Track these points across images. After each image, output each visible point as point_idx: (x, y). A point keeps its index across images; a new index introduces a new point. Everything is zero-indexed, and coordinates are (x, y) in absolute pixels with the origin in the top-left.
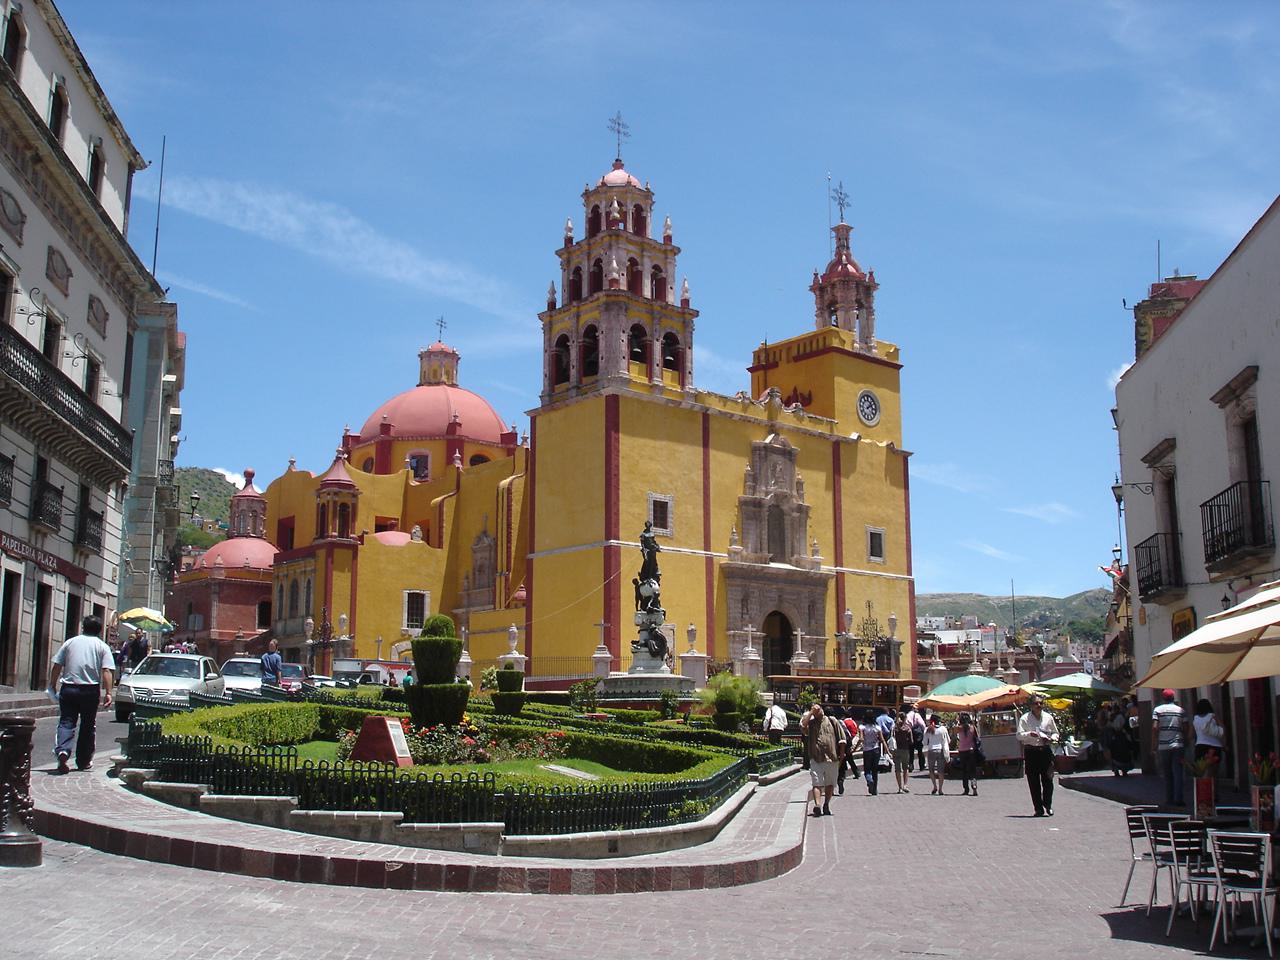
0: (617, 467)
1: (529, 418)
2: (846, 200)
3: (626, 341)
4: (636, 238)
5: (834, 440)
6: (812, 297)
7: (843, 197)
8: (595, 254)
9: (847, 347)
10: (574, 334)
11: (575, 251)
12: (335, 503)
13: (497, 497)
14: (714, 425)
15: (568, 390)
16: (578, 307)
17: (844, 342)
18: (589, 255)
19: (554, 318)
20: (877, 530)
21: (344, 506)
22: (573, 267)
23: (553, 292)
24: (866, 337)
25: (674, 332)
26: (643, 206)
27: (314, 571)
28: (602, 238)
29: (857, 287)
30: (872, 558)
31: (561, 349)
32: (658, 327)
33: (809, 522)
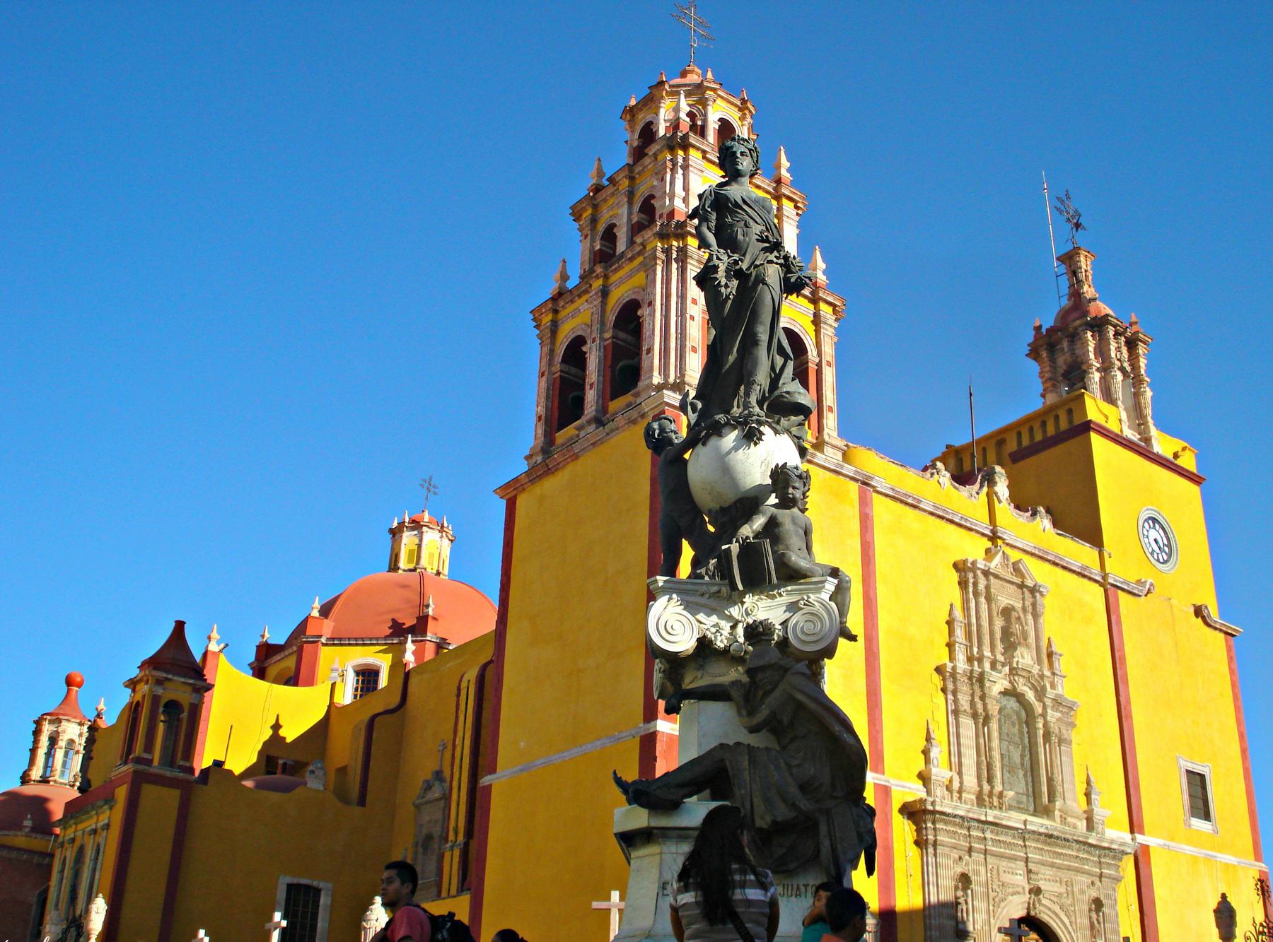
1: (502, 504)
6: (1034, 367)
8: (642, 192)
10: (596, 327)
11: (605, 200)
13: (458, 695)
14: (881, 507)
15: (580, 428)
16: (606, 277)
17: (1107, 417)
18: (631, 195)
19: (562, 314)
21: (173, 707)
22: (601, 228)
23: (564, 277)
25: (796, 330)
27: (107, 826)
28: (655, 156)
29: (1117, 334)
30: (1198, 823)
31: (573, 370)
33: (1075, 736)
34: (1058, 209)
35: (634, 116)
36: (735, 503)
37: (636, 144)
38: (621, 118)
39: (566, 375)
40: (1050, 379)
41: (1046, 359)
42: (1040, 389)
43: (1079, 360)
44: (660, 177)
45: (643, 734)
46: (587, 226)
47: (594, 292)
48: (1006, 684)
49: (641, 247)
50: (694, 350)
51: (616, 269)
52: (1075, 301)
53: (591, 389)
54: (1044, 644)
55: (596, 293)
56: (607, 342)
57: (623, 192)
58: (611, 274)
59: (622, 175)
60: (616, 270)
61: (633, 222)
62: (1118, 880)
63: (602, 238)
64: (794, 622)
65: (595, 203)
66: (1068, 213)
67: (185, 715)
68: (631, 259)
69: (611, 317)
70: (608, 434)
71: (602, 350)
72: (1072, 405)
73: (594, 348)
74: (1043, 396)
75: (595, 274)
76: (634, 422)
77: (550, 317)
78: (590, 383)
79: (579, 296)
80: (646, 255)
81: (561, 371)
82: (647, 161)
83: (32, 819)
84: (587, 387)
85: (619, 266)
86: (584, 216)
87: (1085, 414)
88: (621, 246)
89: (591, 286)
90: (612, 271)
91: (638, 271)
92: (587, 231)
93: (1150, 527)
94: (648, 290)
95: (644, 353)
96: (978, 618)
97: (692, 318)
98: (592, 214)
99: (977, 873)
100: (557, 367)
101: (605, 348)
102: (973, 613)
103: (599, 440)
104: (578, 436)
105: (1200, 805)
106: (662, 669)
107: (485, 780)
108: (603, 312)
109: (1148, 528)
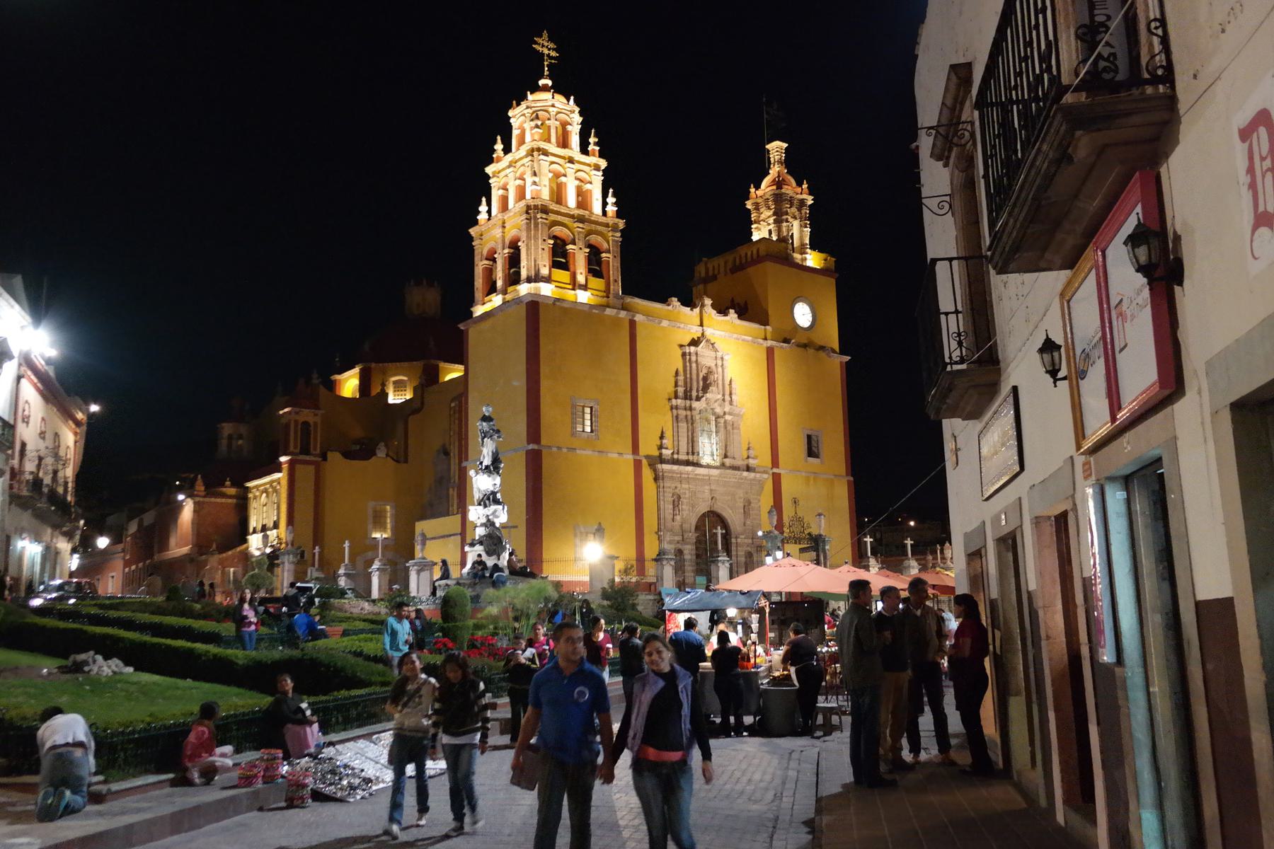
3: (547, 249)
12: (296, 422)
21: (306, 424)
30: (811, 460)
48: (704, 405)
50: (545, 266)
54: (727, 382)
62: (760, 493)
67: (312, 428)
83: (230, 480)
96: (691, 373)
99: (685, 494)
102: (688, 372)
105: (812, 450)
107: (464, 464)
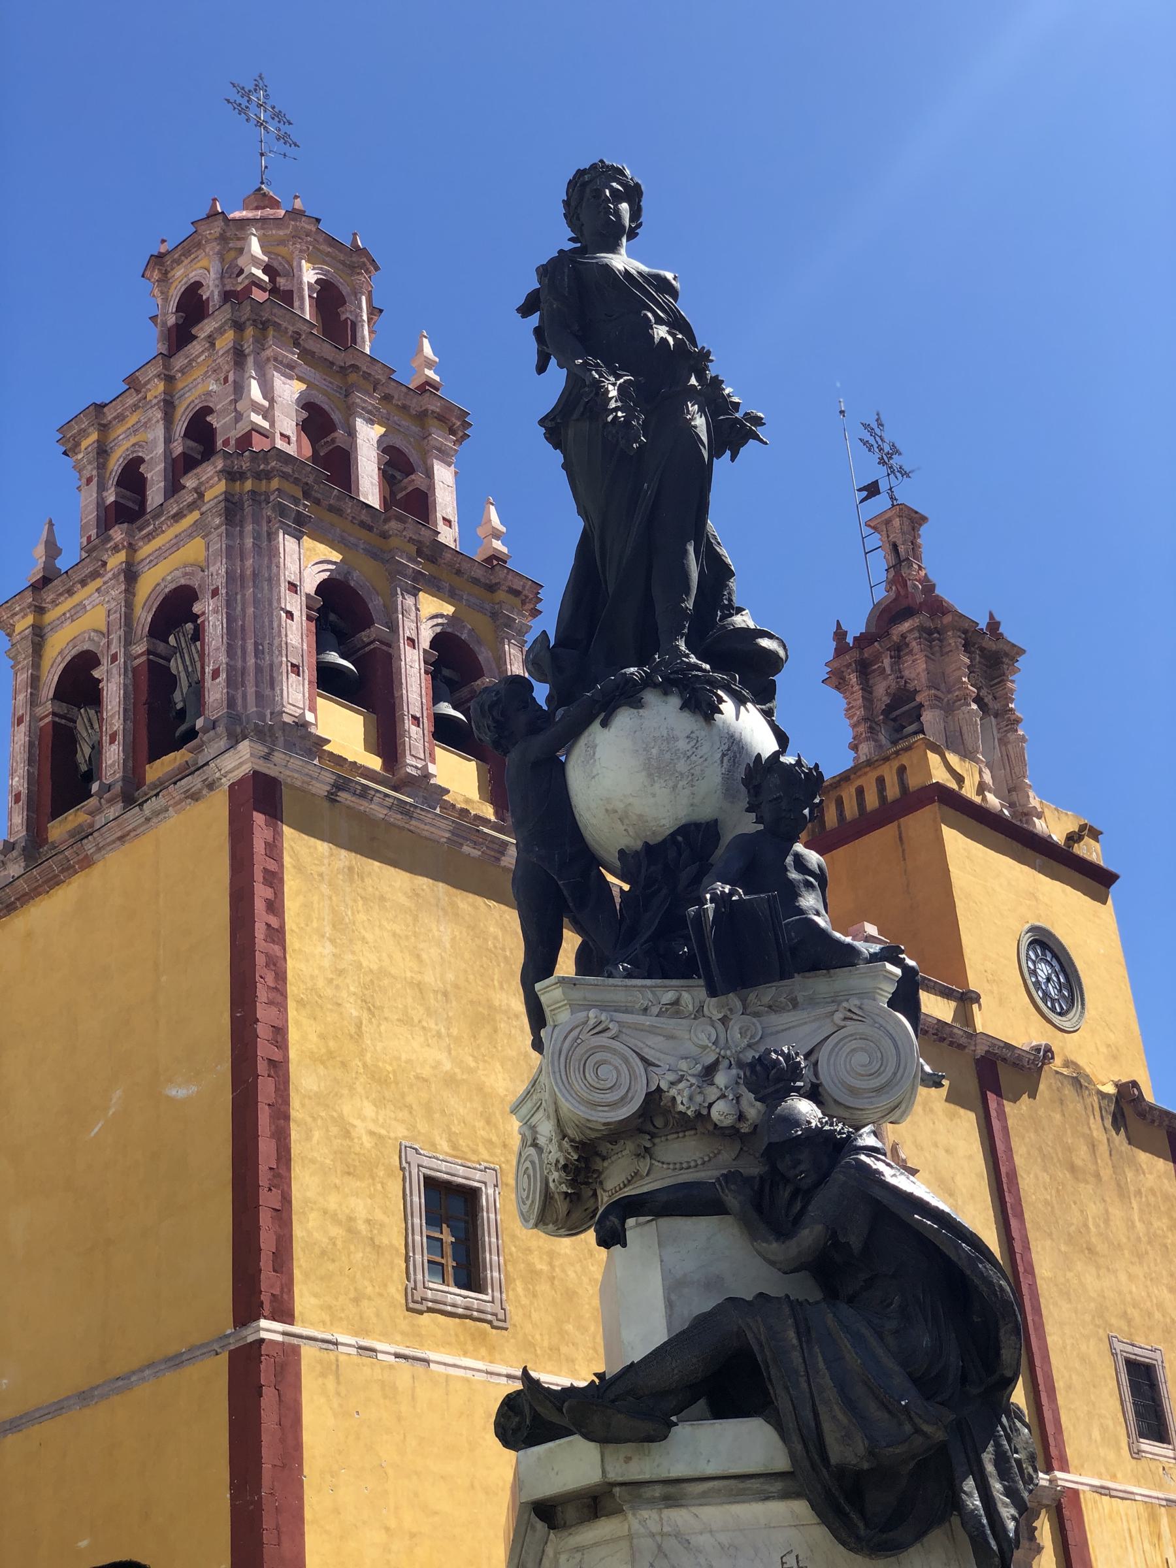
0: (280, 1034)
2: (896, 461)
4: (326, 350)
5: (981, 1051)
6: (836, 701)
7: (887, 448)
9: (969, 791)
11: (121, 418)
16: (132, 548)
17: (960, 779)
18: (169, 406)
19: (51, 616)
20: (1142, 1355)
22: (116, 463)
24: (1012, 790)
26: (345, 290)
28: (211, 340)
30: (1147, 1445)
32: (410, 601)
34: (865, 443)
35: (166, 273)
36: (673, 835)
37: (171, 320)
38: (143, 276)
39: (63, 721)
40: (865, 719)
41: (857, 688)
42: (848, 735)
43: (910, 686)
44: (222, 376)
45: (232, 1347)
46: (90, 463)
47: (110, 575)
49: (195, 495)
50: (296, 669)
51: (150, 534)
52: (898, 593)
53: (112, 741)
55: (115, 576)
56: (138, 661)
57: (155, 401)
58: (141, 544)
59: (152, 371)
60: (150, 537)
61: (174, 456)
63: (119, 484)
64: (583, 1108)
65: (104, 422)
66: (881, 450)
68: (178, 517)
69: (144, 617)
70: (148, 820)
71: (130, 675)
72: (904, 759)
73: (115, 671)
74: (854, 747)
75: (111, 544)
76: (195, 797)
77: (30, 619)
78: (110, 732)
79: (84, 583)
80: (204, 509)
81: (54, 714)
82: (195, 348)
84: (106, 739)
85: (155, 530)
86: (84, 444)
87: (930, 776)
88: (155, 495)
89: (104, 564)
90: (142, 538)
91: (191, 536)
92: (90, 470)
93: (1037, 956)
94: (211, 569)
95: (208, 676)
97: (290, 615)
98: (98, 441)
100: (47, 708)
101: (135, 670)
103: (134, 830)
104: (91, 825)
106: (562, 1162)
108: (129, 605)
109: (1033, 957)
